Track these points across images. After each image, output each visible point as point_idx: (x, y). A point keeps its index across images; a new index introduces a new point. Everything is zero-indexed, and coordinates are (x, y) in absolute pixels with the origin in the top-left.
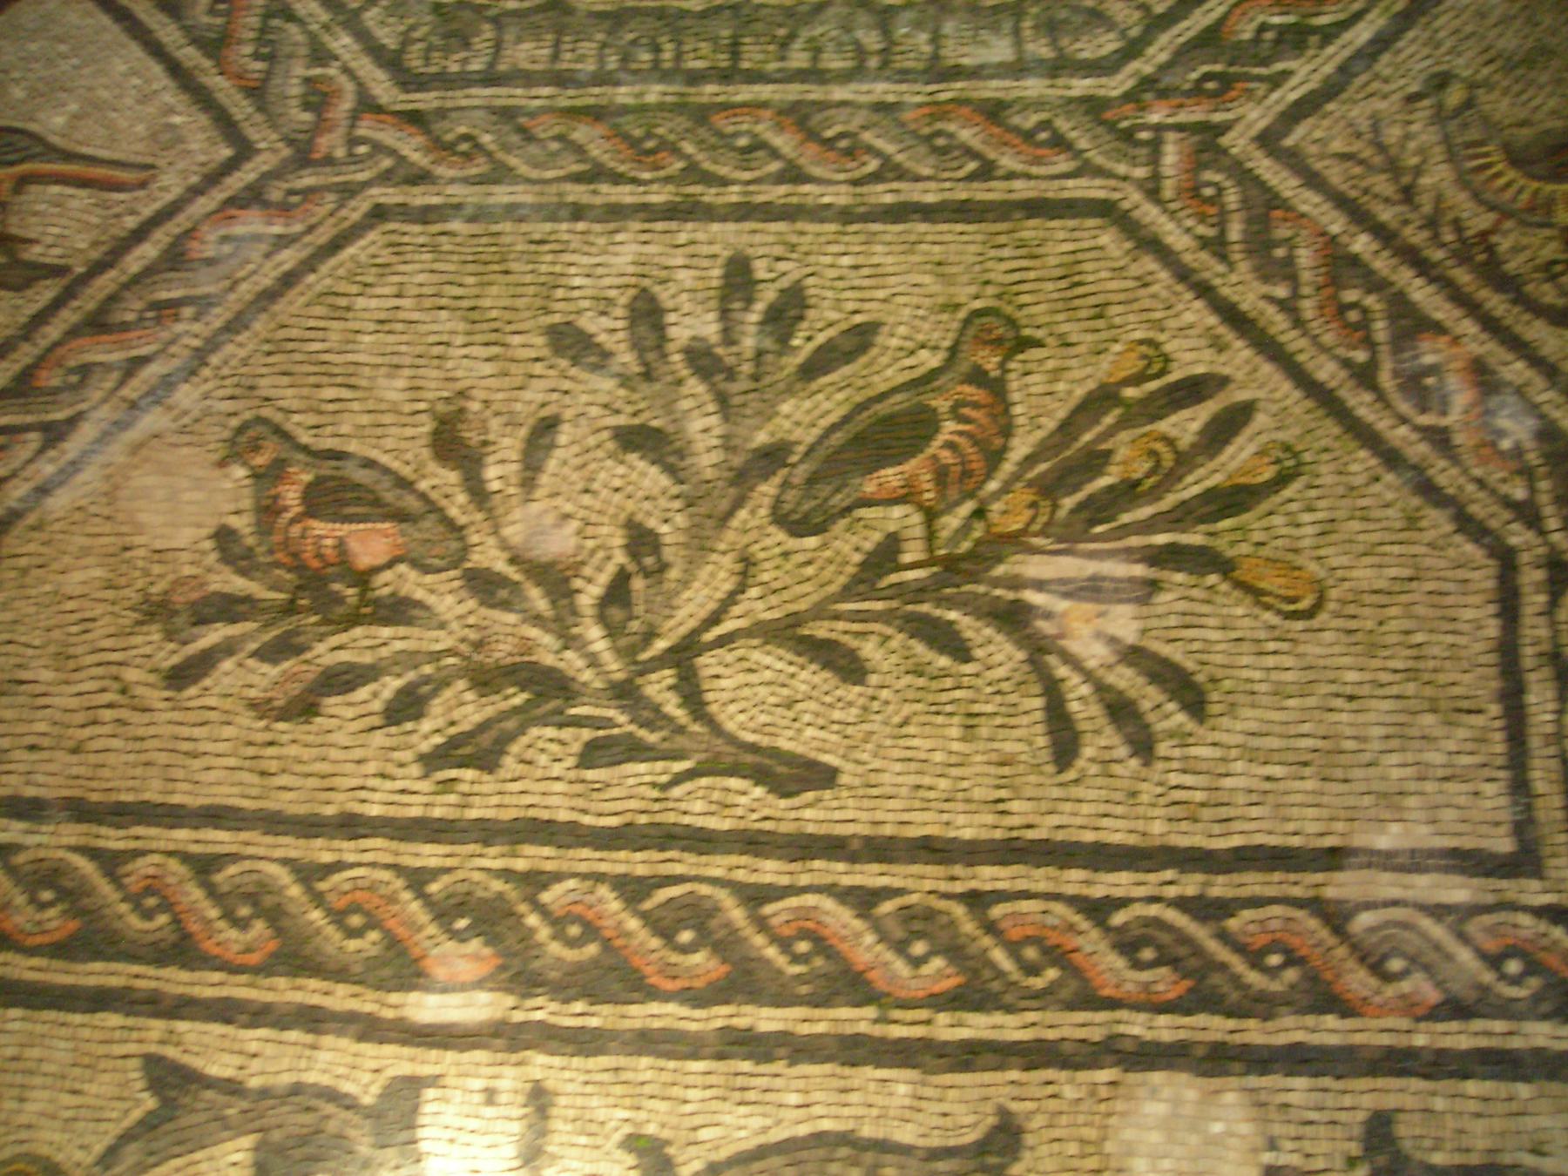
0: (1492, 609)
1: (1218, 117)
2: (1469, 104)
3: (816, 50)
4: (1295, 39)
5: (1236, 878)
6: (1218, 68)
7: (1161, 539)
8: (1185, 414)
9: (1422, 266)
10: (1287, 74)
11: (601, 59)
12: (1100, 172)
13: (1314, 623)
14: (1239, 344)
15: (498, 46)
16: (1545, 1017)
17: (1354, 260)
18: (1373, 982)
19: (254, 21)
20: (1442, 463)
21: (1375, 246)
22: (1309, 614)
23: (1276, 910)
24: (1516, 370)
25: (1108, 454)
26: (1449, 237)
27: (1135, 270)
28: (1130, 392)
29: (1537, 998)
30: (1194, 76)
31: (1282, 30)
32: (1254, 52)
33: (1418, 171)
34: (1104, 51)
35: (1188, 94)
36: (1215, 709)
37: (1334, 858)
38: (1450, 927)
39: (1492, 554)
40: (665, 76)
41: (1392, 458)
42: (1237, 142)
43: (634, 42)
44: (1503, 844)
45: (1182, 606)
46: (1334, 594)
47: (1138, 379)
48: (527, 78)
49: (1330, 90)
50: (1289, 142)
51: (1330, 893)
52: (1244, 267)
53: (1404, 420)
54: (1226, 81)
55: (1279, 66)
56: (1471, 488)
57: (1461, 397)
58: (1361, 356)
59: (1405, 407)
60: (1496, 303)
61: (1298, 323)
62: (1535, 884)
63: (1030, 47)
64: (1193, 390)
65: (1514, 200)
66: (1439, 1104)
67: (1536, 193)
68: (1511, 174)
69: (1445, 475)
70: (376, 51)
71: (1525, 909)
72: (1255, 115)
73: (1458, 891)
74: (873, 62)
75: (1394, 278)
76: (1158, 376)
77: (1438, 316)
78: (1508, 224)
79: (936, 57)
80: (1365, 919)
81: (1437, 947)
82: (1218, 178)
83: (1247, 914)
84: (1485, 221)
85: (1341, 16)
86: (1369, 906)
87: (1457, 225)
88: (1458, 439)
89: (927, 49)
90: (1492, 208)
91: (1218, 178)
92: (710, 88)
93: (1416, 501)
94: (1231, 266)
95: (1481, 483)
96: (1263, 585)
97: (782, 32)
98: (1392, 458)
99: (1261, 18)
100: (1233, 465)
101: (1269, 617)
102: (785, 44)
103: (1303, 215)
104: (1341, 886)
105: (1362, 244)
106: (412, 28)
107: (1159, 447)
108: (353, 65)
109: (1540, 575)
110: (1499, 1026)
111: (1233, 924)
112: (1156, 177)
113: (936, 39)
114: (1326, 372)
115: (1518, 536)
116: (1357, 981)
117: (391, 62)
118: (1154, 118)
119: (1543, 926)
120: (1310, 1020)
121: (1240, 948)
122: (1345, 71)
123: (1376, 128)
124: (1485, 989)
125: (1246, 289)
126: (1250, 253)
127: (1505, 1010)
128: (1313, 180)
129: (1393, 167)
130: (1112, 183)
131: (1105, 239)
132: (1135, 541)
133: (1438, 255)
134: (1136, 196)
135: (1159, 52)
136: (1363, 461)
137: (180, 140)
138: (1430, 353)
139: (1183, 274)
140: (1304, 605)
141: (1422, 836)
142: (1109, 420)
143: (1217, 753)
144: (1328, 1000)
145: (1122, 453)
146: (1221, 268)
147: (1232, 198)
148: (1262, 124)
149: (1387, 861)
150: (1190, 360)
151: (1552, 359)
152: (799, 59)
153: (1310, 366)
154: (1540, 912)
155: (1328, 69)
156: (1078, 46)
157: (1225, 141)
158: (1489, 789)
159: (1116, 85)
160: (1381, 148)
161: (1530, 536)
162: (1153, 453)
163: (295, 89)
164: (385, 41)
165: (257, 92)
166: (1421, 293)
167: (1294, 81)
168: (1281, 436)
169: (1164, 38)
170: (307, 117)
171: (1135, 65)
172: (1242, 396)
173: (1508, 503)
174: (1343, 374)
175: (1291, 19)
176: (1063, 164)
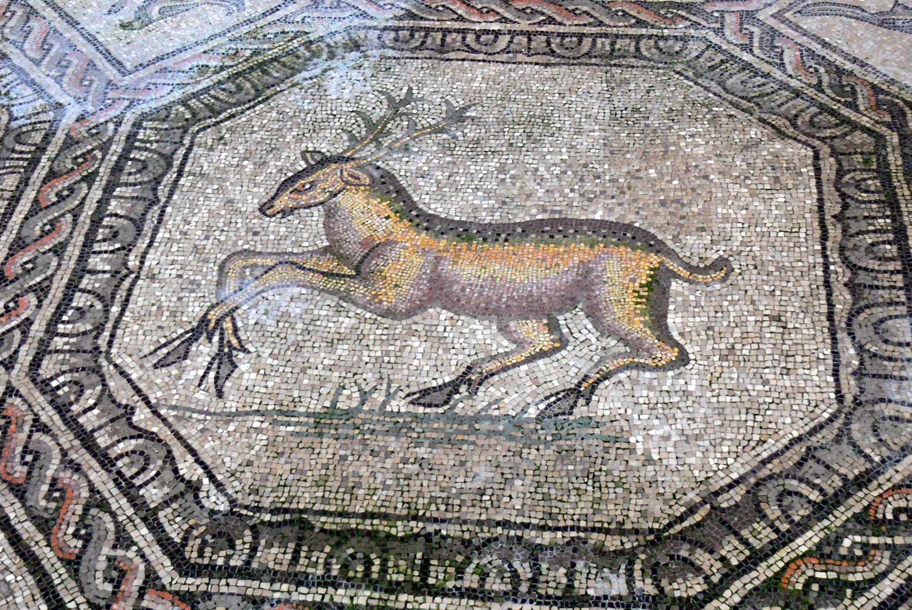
3: (484, 576)
11: (327, 565)
15: (254, 549)
19: (79, 509)
31: (823, 584)
34: (692, 593)
40: (373, 585)
43: (353, 556)
48: (275, 577)
63: (638, 584)
70: (164, 542)
74: (524, 588)
79: (570, 587)
85: (870, 575)
89: (564, 580)
92: (403, 597)
97: (460, 558)
99: (810, 573)
102: (460, 572)
106: (192, 527)
108: (147, 551)
113: (570, 576)
117: (174, 552)
137: (11, 593)
152: (470, 580)
156: (675, 586)
163: (102, 564)
164: (173, 535)
165: (73, 564)
169: (738, 584)
170: (109, 587)
175: (832, 575)
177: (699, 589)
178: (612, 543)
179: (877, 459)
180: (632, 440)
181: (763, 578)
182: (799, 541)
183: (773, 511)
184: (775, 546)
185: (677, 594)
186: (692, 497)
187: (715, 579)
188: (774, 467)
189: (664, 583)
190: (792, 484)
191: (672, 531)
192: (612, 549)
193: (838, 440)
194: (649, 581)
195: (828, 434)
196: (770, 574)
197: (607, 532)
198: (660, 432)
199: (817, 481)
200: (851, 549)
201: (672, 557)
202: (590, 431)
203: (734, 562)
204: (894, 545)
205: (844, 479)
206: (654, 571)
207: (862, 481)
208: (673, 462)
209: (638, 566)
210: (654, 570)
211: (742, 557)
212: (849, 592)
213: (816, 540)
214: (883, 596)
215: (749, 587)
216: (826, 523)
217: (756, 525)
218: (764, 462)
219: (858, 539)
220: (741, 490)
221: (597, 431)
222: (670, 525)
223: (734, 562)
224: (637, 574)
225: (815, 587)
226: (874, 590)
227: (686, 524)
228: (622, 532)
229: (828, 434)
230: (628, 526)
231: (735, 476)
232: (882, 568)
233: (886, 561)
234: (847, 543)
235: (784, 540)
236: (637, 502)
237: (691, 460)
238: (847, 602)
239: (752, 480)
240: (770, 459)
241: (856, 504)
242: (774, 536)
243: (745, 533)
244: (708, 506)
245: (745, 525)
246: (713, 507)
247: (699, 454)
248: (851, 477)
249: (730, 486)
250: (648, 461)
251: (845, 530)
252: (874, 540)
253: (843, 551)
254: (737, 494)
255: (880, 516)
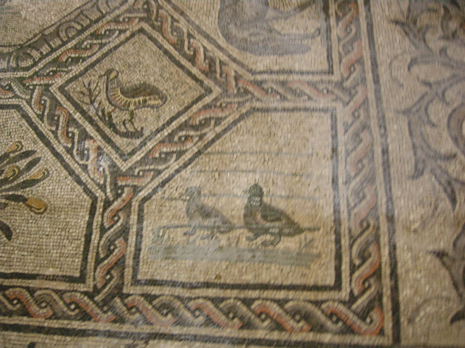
0: (88, 213)
1: (50, 82)
2: (116, 77)
4: (76, 61)
5: (10, 280)
6: (55, 69)
7: (10, 193)
8: (24, 160)
9: (91, 121)
10: (71, 70)
12: (19, 97)
13: (43, 216)
14: (40, 142)
16: (79, 320)
17: (74, 120)
18: (37, 309)
20: (84, 174)
21: (80, 116)
22: (42, 213)
23: (18, 289)
24: (108, 149)
25: (3, 171)
26: (100, 114)
27: (20, 123)
28: (12, 155)
29: (76, 315)
30: (48, 71)
31: (72, 59)
32: (65, 64)
33: (97, 95)
34: (27, 65)
35: (45, 76)
36: (13, 237)
37: (33, 277)
38: (59, 295)
39: (91, 198)
41: (71, 173)
42: (53, 89)
44: (77, 275)
45: (11, 210)
46: (49, 208)
47: (14, 152)
49: (82, 74)
50: (66, 89)
51: (31, 285)
52: (46, 122)
53: (76, 162)
54: (55, 72)
55: (70, 68)
56: (89, 180)
57: (92, 156)
58: (70, 145)
59: (77, 159)
60: (108, 131)
61: (56, 137)
62: (82, 285)
63: (11, 64)
64: (27, 154)
65: (121, 102)
66: (47, 341)
67: (127, 101)
68: (121, 96)
69: (84, 177)
71: (79, 292)
72: (59, 81)
73: (63, 286)
75: (83, 125)
76: (20, 150)
77: (92, 135)
78: (117, 110)
80: (39, 293)
81: (55, 300)
82: (46, 98)
83: (11, 290)
84: (111, 108)
86: (40, 289)
87: (103, 111)
88: (89, 168)
90: (112, 105)
91: (46, 98)
93: (75, 184)
94: (43, 122)
95: (92, 179)
96: (33, 205)
98: (71, 173)
100: (32, 174)
101: (32, 214)
103: (64, 108)
104: (33, 284)
105: (77, 116)
107: (16, 169)
109: (102, 204)
110: (66, 322)
111: (7, 292)
112: (31, 97)
114: (60, 150)
115: (99, 193)
116: (34, 308)
118: (35, 83)
119: (82, 296)
120: (20, 318)
121: (8, 299)
122: (86, 70)
123: (89, 84)
124: (64, 312)
125: (45, 127)
126: (48, 118)
127: (69, 318)
128: (69, 99)
129: (91, 95)
130: (20, 100)
131: (15, 115)
132: (4, 193)
133: (96, 118)
134: (25, 103)
135: (41, 65)
136: (65, 172)
138: (88, 144)
139: (31, 123)
140: (41, 211)
141: (58, 272)
142: (5, 162)
143: (12, 248)
144: (26, 313)
145: (7, 170)
146: (41, 122)
147: (48, 104)
148: (60, 85)
149: (47, 278)
150: (28, 146)
151: (119, 146)
153: (56, 148)
154: (82, 293)
155: (82, 69)
157: (50, 88)
158: (77, 260)
159: (27, 74)
160: (90, 90)
161: (102, 193)
162: (14, 170)
166: (89, 128)
167: (73, 71)
168: (45, 166)
169: (44, 61)
171: (35, 68)
172: (37, 156)
173: (98, 185)
174: (64, 150)
175: (77, 55)
176: (10, 95)
177: (30, 63)
178: (6, 50)
179: (104, 12)
180: (22, 13)
181: (53, 58)
182: (69, 44)
183: (63, 34)
184: (60, 46)
185: (23, 66)
186: (37, 31)
187: (36, 60)
188: (67, 19)
189: (19, 62)
190: (73, 24)
191: (27, 44)
192: (5, 52)
193: (93, 6)
194: (14, 62)
195: (90, 5)
196: (55, 56)
197: (5, 46)
198: (32, 9)
199: (81, 22)
200: (86, 46)
201: (24, 53)
202: (8, 11)
203: (44, 53)
204: (102, 43)
205: (91, 20)
206: (17, 59)
207: (97, 21)
208: (33, 19)
209: (12, 58)
210: (17, 58)
211: (47, 51)
212: (81, 61)
213: (75, 43)
214: (92, 61)
215: (47, 61)
216: (80, 37)
217: (55, 40)
218: (64, 17)
219: (89, 41)
220: (54, 28)
221: (11, 11)
222: (27, 42)
223: (44, 53)
224: (11, 60)
225: (70, 60)
226: (90, 59)
227: (32, 41)
228: (10, 46)
229: (90, 5)
230: (13, 44)
231: (53, 23)
232: (95, 51)
233: (97, 49)
234: (85, 43)
235: (64, 43)
236: (18, 34)
237: (40, 18)
238: (79, 64)
239: (59, 24)
240: (67, 16)
241: (92, 30)
242: (61, 43)
243: (51, 43)
244: (41, 34)
245: (50, 40)
246: (43, 35)
247: (43, 16)
248: (93, 19)
249: (50, 27)
250: (25, 19)
251: (86, 39)
252: (95, 42)
253: (83, 46)
254: (51, 30)
255: (99, 33)
